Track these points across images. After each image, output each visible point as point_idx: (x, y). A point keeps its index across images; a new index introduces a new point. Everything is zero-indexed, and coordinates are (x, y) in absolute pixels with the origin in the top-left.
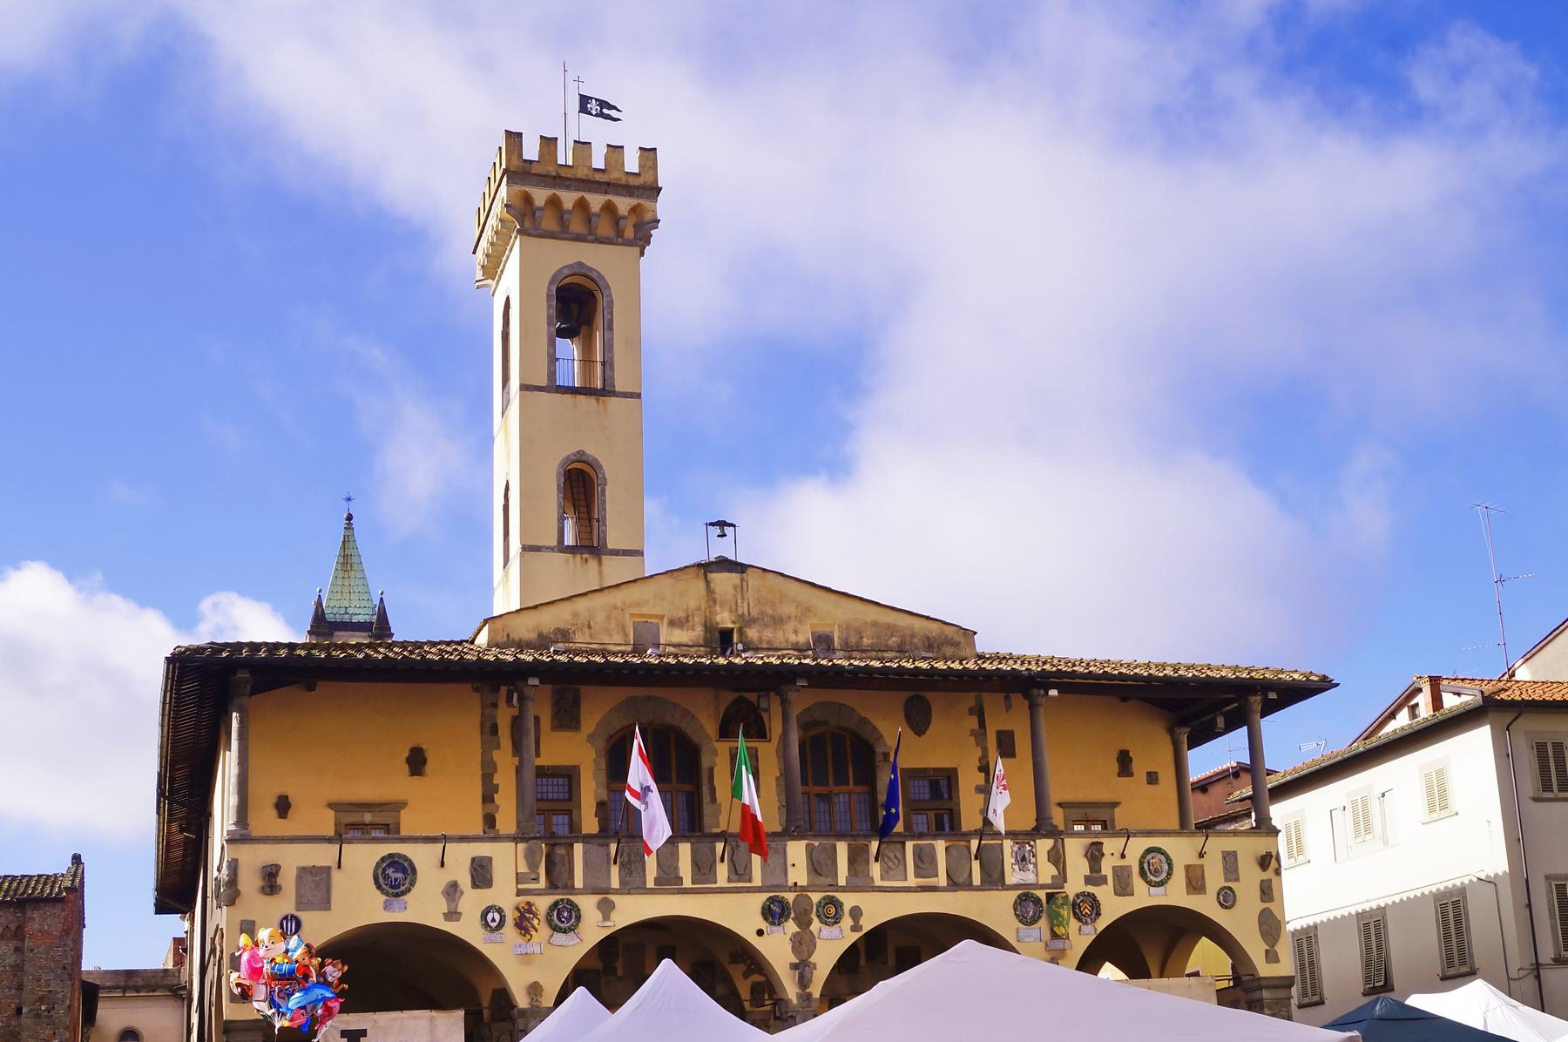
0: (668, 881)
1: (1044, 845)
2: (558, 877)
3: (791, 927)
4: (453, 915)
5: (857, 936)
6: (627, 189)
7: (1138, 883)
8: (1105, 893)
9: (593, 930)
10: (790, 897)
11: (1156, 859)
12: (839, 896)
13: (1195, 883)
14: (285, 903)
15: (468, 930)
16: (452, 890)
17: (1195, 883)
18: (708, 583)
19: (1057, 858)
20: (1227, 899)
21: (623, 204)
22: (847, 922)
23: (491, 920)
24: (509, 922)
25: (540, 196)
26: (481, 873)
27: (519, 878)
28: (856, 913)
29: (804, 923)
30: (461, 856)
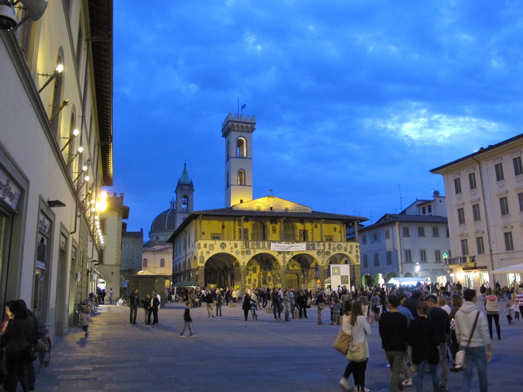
0: (264, 247)
1: (322, 244)
2: (247, 246)
3: (282, 255)
4: (232, 252)
6: (250, 123)
7: (336, 250)
8: (331, 251)
9: (253, 254)
11: (339, 246)
13: (346, 250)
14: (207, 249)
15: (234, 254)
16: (232, 248)
17: (346, 250)
19: (324, 245)
20: (351, 252)
21: (249, 126)
25: (235, 124)
26: (236, 246)
27: (241, 246)
30: (233, 243)
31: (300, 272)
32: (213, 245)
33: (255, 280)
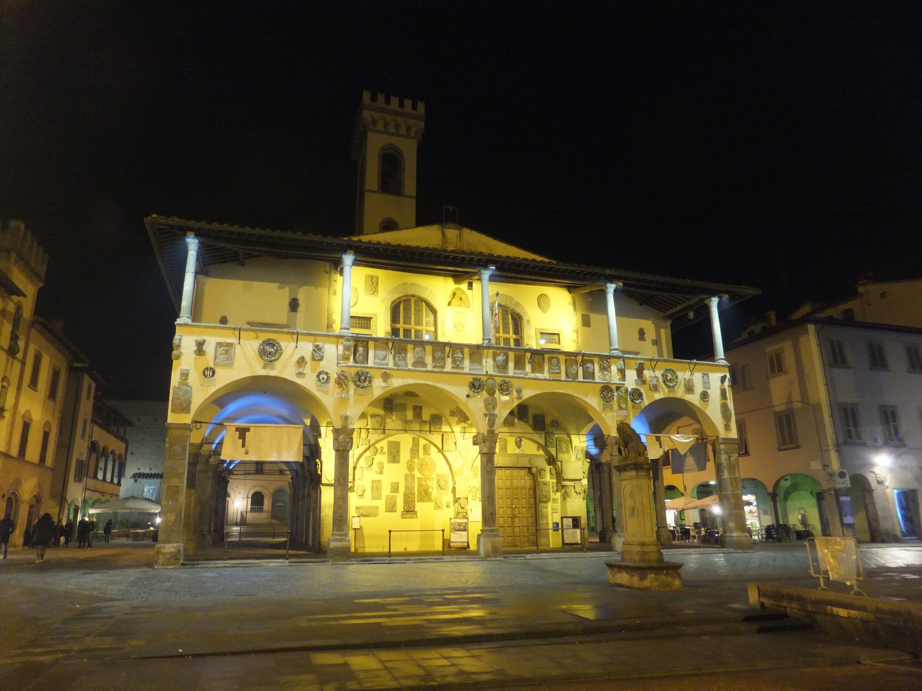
3: (485, 394)
10: (484, 378)
15: (309, 383)
18: (443, 234)
23: (322, 378)
24: (332, 380)
28: (519, 391)
29: (491, 393)
31: (542, 463)
32: (230, 345)
33: (395, 488)
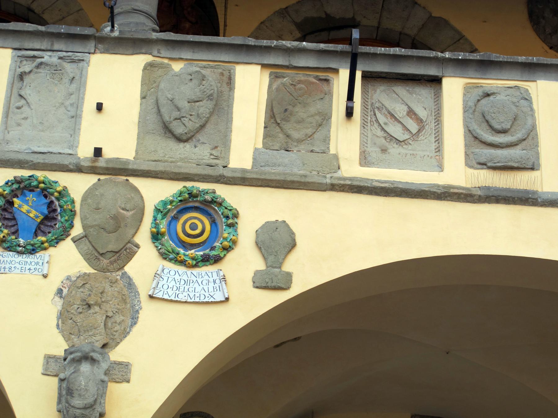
3: (66, 259)
5: (273, 300)
10: (77, 186)
12: (223, 192)
22: (245, 260)
28: (277, 242)
